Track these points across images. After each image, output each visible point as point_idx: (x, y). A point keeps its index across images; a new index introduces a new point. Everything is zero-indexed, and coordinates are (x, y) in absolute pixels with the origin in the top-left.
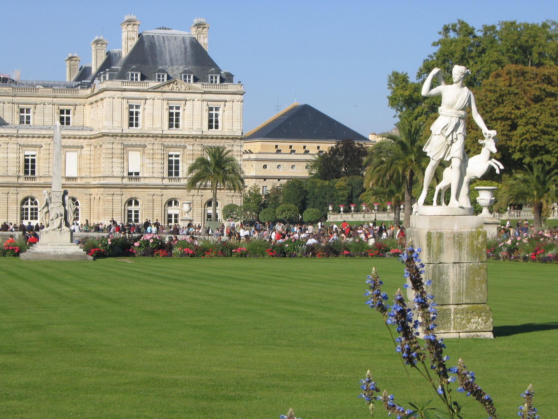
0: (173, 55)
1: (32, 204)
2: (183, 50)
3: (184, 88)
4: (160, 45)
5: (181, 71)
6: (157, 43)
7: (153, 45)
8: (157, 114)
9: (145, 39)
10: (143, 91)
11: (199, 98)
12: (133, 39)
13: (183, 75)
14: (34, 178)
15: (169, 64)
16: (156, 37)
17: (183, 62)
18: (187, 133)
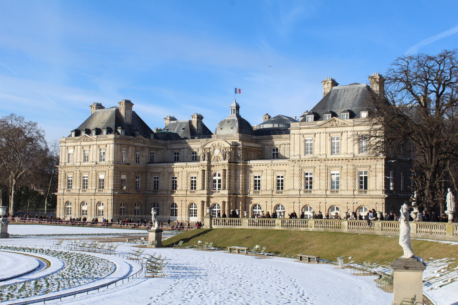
0: (346, 100)
1: (259, 209)
2: (354, 97)
3: (340, 124)
4: (340, 95)
6: (339, 94)
7: (336, 95)
8: (323, 144)
9: (332, 92)
10: (313, 128)
11: (350, 130)
14: (281, 192)
15: (341, 107)
16: (340, 90)
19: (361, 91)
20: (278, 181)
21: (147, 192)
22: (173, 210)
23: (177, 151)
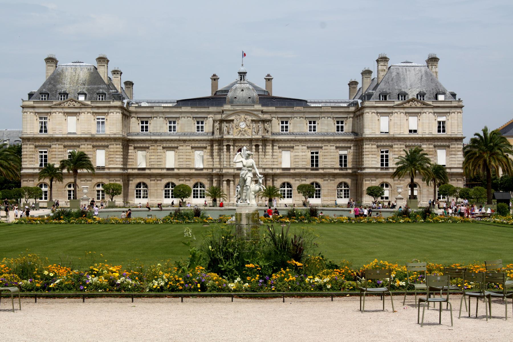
5: (418, 93)
6: (401, 73)
12: (384, 70)
13: (419, 96)
14: (317, 169)
15: (409, 87)
17: (419, 85)
18: (421, 136)
19: (423, 72)
20: (312, 157)
21: (130, 171)
22: (169, 191)
23: (145, 120)
